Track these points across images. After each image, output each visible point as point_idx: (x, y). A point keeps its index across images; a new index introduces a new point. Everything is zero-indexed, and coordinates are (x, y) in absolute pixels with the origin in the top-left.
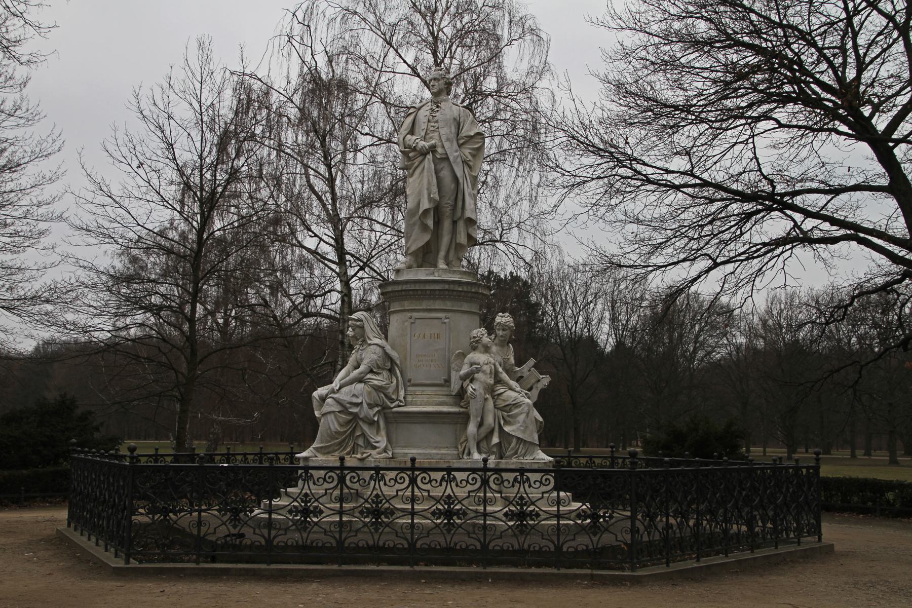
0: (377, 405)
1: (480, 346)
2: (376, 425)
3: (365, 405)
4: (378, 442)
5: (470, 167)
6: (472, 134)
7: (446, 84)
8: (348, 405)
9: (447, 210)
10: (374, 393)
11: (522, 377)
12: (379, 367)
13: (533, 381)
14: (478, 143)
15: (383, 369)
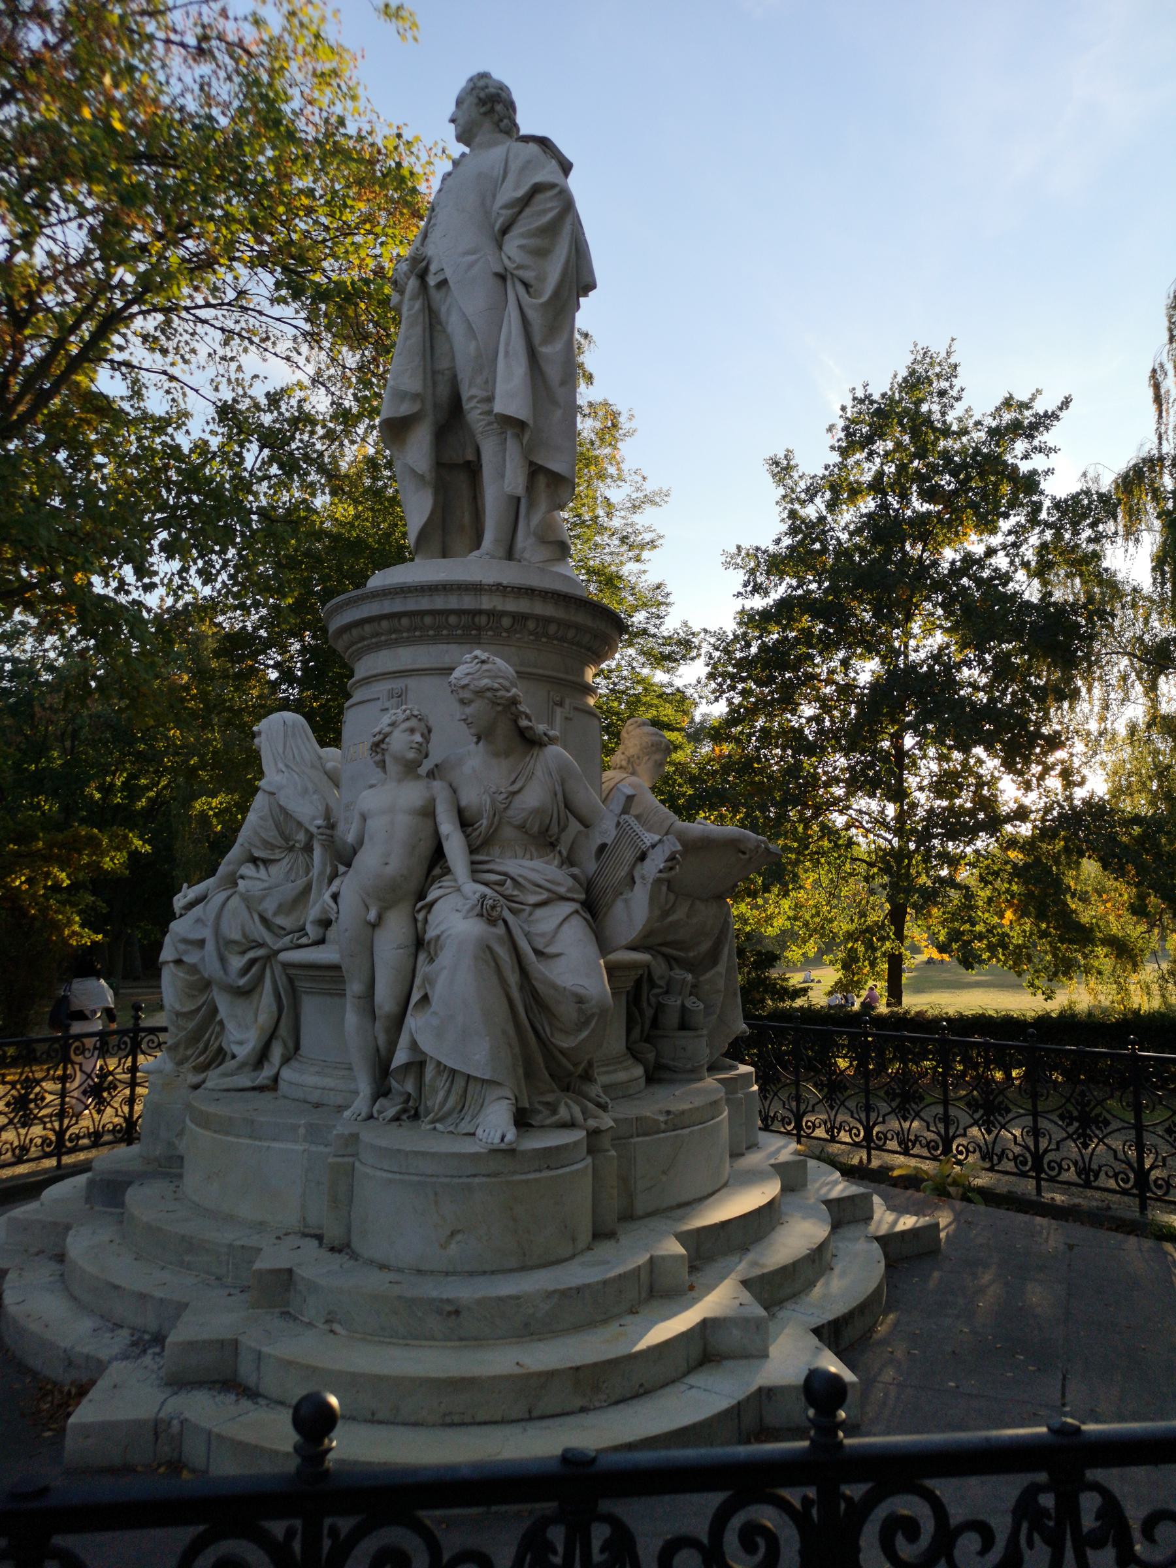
0: (261, 945)
1: (388, 759)
2: (256, 996)
3: (210, 946)
4: (240, 1043)
5: (526, 285)
6: (520, 193)
7: (482, 102)
8: (182, 947)
9: (474, 414)
10: (245, 913)
11: (603, 847)
12: (272, 847)
13: (630, 855)
14: (544, 212)
15: (291, 849)
